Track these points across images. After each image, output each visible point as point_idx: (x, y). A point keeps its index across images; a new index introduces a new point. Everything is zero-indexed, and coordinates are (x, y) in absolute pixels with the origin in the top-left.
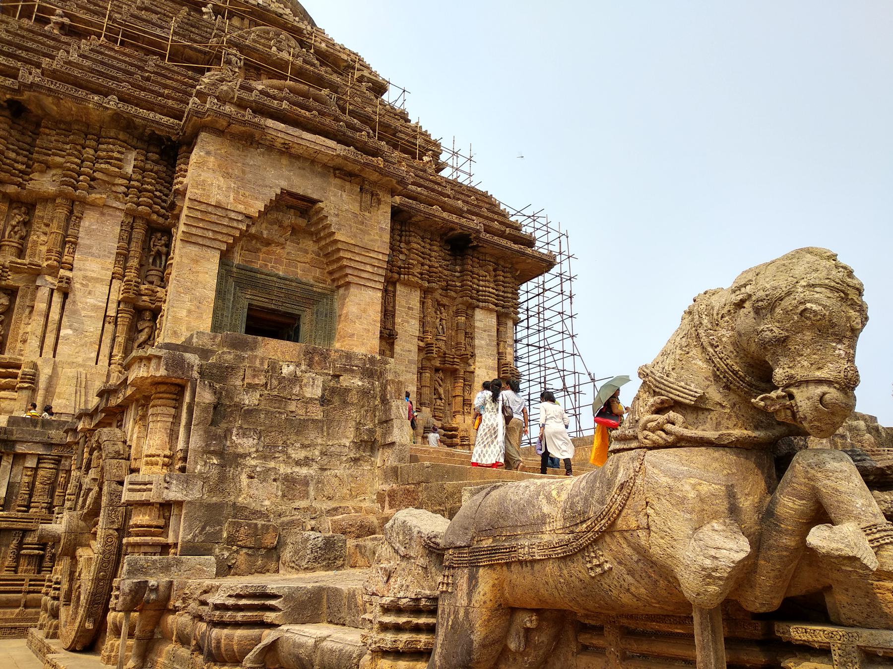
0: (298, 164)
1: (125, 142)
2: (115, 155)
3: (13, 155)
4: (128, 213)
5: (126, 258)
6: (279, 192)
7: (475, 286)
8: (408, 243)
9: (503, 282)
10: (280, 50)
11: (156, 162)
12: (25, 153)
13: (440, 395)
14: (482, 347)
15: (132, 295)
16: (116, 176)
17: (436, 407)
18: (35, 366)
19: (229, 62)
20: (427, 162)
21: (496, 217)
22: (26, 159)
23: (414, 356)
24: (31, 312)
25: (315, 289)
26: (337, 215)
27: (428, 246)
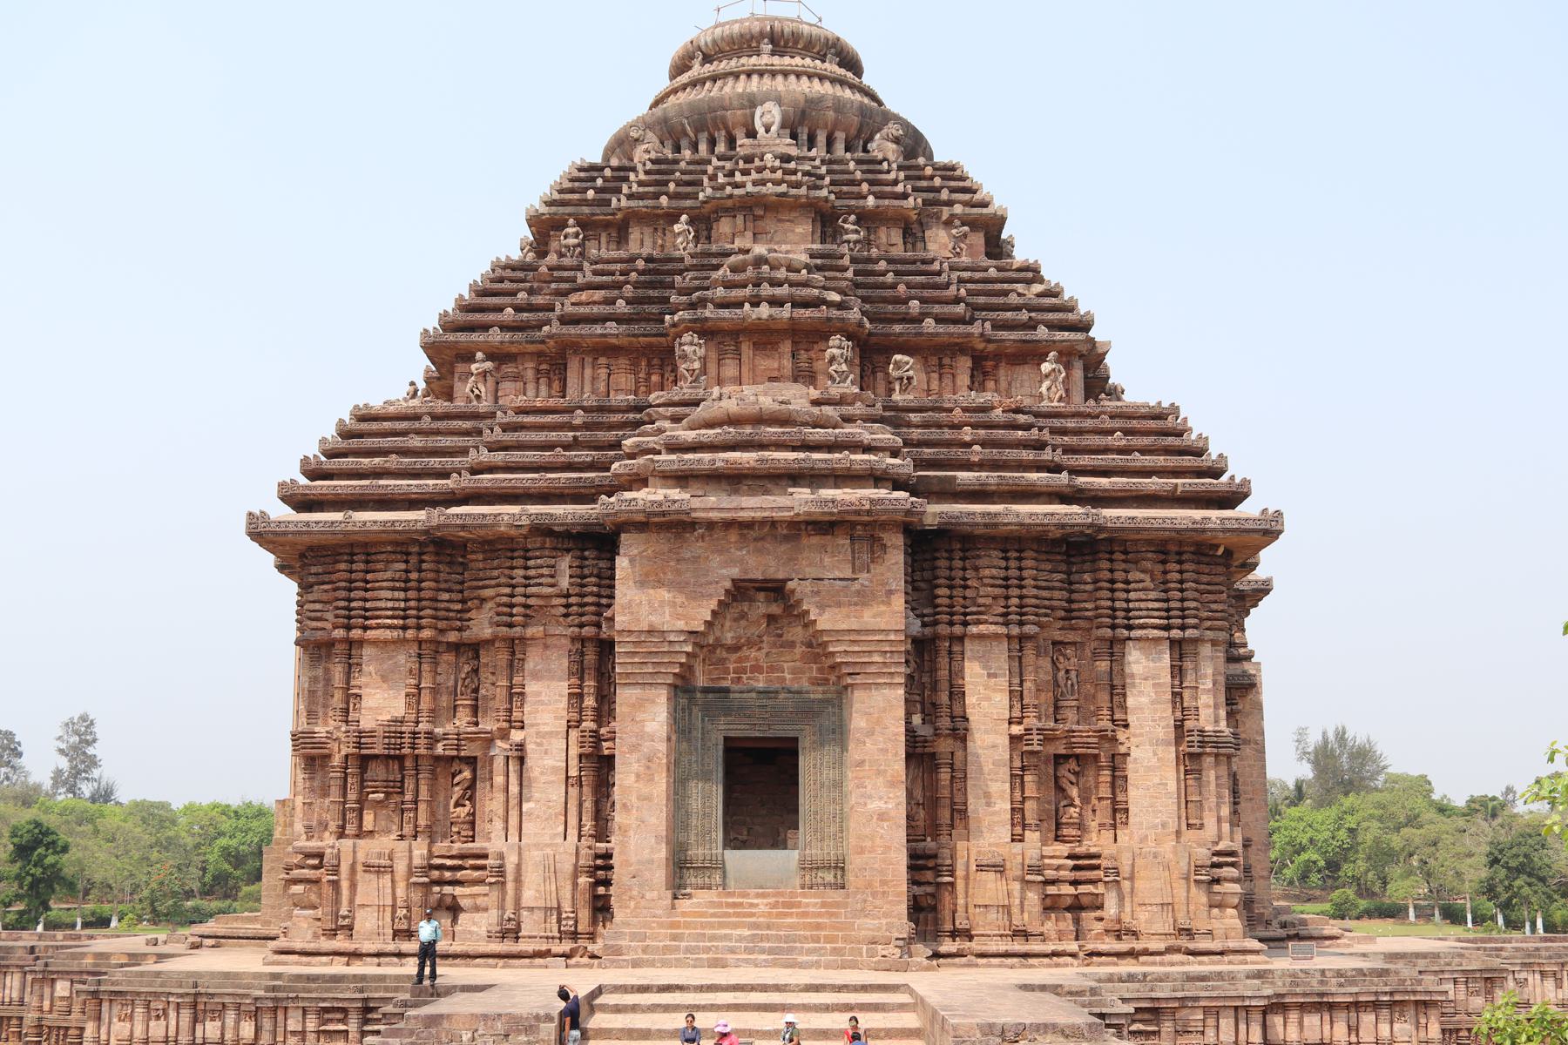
0: (752, 534)
1: (555, 549)
2: (545, 571)
3: (446, 596)
4: (573, 639)
5: (580, 696)
6: (728, 584)
7: (1118, 604)
8: (976, 569)
9: (1181, 582)
10: (755, 304)
11: (598, 559)
12: (459, 587)
13: (1073, 800)
14: (1142, 709)
15: (588, 750)
16: (549, 597)
17: (1064, 820)
18: (501, 856)
19: (685, 357)
20: (1047, 376)
21: (1160, 461)
22: (460, 596)
23: (1003, 752)
24: (492, 786)
25: (812, 696)
26: (818, 593)
27: (1013, 564)
